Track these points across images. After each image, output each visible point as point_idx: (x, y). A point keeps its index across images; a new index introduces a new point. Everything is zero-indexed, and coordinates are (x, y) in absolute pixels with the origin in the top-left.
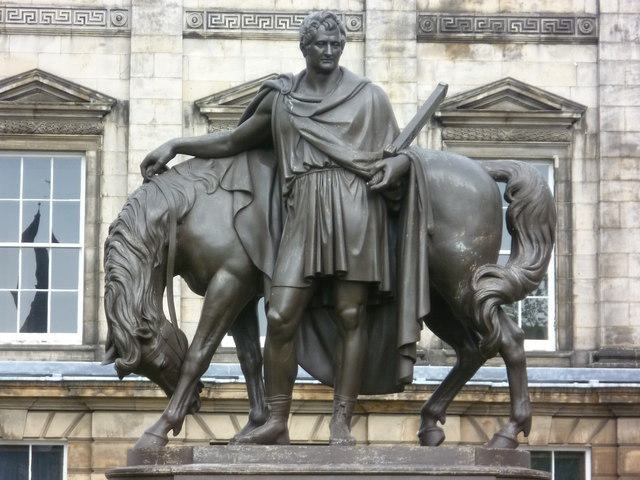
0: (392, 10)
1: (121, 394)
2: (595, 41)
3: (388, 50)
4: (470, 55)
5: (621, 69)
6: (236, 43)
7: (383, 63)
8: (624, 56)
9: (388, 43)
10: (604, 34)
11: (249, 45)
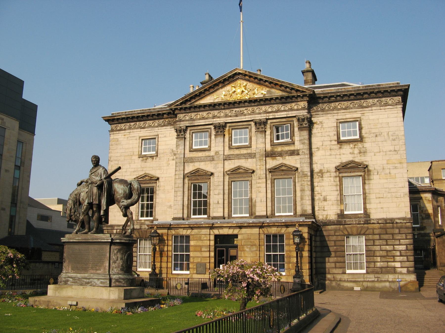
0: (261, 152)
1: (197, 226)
2: (299, 155)
3: (260, 159)
4: (276, 159)
5: (304, 159)
6: (233, 160)
7: (259, 162)
8: (304, 157)
9: (260, 158)
10: (300, 153)
11: (236, 161)
